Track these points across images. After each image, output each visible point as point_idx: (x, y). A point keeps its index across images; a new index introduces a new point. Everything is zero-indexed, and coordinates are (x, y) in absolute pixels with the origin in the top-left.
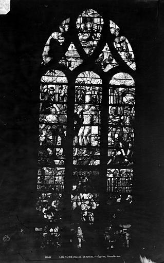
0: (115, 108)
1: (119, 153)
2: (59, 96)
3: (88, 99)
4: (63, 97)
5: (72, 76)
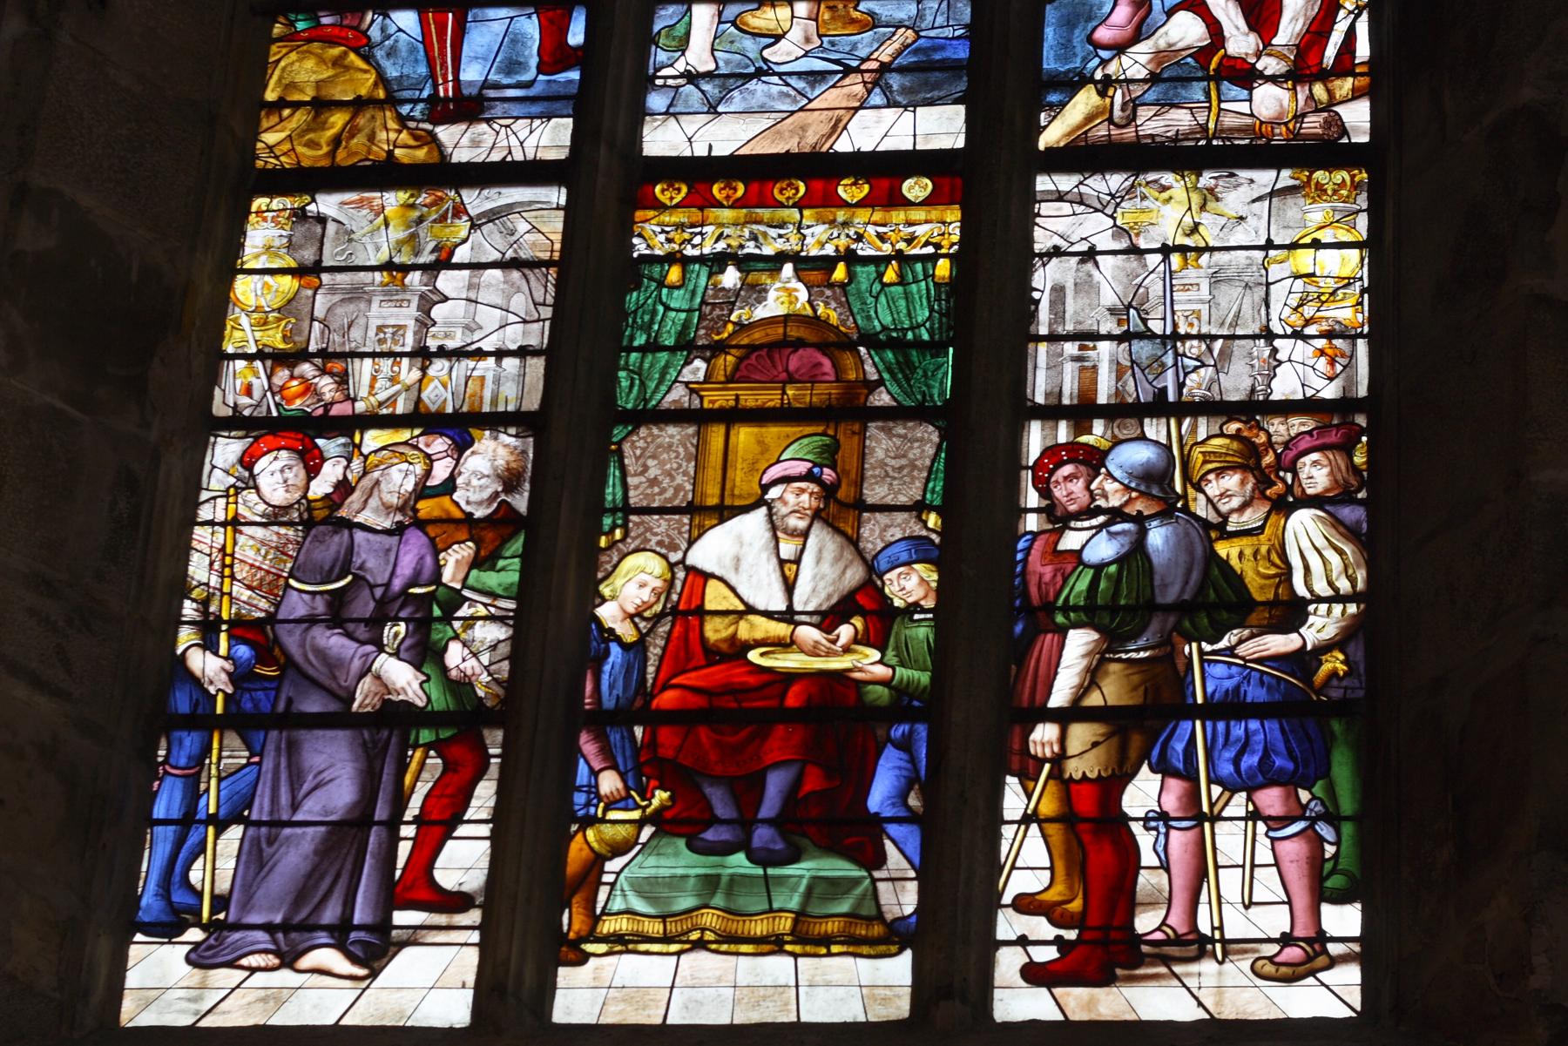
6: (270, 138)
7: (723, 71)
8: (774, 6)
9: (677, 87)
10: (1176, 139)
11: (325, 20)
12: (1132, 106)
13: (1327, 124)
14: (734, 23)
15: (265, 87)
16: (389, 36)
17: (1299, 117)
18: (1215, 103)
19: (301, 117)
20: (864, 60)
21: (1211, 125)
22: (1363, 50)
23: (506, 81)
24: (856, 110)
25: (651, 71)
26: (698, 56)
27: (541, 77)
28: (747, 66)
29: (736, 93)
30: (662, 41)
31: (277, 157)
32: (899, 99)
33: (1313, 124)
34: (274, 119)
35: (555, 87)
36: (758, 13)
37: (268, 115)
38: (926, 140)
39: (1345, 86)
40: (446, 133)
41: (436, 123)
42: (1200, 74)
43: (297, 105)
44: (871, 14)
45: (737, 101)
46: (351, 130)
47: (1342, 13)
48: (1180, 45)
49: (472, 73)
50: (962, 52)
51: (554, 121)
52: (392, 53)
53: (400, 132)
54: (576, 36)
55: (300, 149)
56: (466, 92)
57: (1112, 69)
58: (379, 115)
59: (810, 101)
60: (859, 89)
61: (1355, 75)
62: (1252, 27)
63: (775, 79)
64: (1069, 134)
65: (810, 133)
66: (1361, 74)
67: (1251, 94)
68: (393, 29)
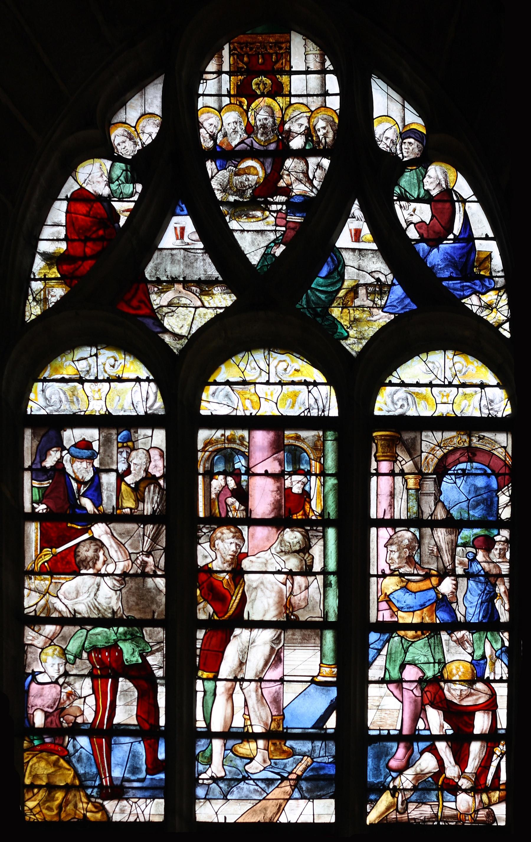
0: (406, 535)
1: (427, 763)
2: (121, 478)
3: (263, 498)
4: (138, 490)
6: (31, 804)
7: (229, 777)
8: (248, 742)
9: (209, 785)
10: (424, 821)
11: (47, 740)
12: (406, 802)
14: (231, 750)
15: (24, 776)
16: (77, 751)
17: (476, 811)
18: (441, 803)
19: (42, 794)
20: (290, 773)
21: (439, 814)
23: (133, 778)
24: (288, 800)
25: (197, 775)
26: (216, 769)
27: (148, 777)
28: (239, 775)
29: (235, 789)
31: (34, 815)
32: (306, 795)
34: (31, 794)
35: (155, 782)
36: (242, 745)
37: (27, 792)
38: (319, 818)
39: (495, 795)
40: (109, 805)
41: (104, 800)
42: (434, 787)
43: (40, 787)
44: (292, 748)
45: (235, 794)
46: (65, 802)
47: (495, 757)
48: (426, 771)
49: (117, 773)
50: (332, 771)
51: (156, 800)
52: (79, 760)
53: (88, 804)
54: (161, 755)
55: (44, 811)
56: (115, 783)
57: (397, 782)
58: (78, 794)
59: (268, 794)
60: (288, 789)
61: (500, 790)
62: (457, 762)
63: (251, 782)
64: (379, 817)
65: (268, 812)
66: (503, 790)
67: (456, 798)
68: (78, 747)
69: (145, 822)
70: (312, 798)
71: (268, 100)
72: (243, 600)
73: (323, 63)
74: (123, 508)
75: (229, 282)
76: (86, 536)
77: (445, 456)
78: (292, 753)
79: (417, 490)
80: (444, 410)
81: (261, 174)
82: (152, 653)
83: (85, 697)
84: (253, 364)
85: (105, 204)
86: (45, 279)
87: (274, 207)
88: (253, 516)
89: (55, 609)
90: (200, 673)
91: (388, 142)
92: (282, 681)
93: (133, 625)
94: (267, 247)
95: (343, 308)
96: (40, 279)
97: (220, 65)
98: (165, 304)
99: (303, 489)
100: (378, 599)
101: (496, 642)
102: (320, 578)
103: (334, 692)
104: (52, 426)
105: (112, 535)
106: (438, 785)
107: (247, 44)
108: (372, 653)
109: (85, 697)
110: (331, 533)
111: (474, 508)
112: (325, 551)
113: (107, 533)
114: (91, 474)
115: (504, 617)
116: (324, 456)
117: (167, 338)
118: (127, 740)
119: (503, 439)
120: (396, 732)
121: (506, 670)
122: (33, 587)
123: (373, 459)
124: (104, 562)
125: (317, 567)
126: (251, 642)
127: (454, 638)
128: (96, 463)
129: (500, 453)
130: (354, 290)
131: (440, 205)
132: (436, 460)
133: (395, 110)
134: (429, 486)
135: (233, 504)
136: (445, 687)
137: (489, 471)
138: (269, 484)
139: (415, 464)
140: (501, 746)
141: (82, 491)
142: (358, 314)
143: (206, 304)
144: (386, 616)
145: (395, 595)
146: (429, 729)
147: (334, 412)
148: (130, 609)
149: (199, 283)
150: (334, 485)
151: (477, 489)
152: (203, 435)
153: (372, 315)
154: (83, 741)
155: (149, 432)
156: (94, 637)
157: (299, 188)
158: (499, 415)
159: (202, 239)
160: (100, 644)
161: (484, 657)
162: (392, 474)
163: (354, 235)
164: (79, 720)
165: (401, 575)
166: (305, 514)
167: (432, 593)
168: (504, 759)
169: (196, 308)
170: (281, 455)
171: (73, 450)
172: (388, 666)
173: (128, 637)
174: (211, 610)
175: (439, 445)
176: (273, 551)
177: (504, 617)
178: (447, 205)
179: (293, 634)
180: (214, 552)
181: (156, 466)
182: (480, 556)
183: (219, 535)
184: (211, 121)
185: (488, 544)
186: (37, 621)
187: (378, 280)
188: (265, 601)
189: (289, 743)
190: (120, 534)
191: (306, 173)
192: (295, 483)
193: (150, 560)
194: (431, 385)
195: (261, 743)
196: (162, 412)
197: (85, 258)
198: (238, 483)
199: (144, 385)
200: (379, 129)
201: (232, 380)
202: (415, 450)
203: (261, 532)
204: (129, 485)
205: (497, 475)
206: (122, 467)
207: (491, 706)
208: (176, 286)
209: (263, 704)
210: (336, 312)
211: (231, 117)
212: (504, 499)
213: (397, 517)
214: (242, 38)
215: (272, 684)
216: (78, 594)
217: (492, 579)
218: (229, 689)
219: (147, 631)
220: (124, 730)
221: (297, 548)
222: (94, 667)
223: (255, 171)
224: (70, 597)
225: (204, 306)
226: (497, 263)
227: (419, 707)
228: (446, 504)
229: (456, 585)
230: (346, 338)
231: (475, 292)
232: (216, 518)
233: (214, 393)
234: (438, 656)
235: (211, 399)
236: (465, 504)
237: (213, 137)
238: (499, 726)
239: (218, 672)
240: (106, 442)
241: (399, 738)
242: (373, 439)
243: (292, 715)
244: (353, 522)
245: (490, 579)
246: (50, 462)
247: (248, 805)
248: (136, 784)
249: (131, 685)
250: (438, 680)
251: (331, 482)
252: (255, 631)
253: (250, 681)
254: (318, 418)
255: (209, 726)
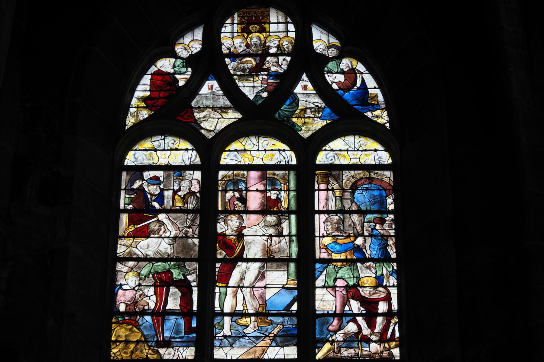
0: (335, 218)
1: (352, 327)
2: (175, 193)
3: (254, 201)
4: (184, 199)
5: (210, 150)
11: (126, 318)
12: (339, 348)
13: (389, 354)
14: (235, 322)
17: (382, 352)
19: (122, 345)
22: (397, 334)
23: (176, 336)
24: (269, 347)
26: (227, 331)
29: (237, 342)
30: (217, 327)
33: (385, 354)
34: (115, 346)
37: (113, 344)
39: (393, 344)
40: (162, 351)
43: (120, 342)
44: (271, 320)
46: (135, 349)
47: (391, 324)
48: (351, 332)
49: (167, 334)
50: (295, 332)
54: (194, 324)
57: (334, 337)
60: (269, 341)
61: (395, 341)
63: (247, 338)
69: (183, 359)
70: (283, 346)
71: (258, 34)
72: (243, 249)
73: (286, 19)
74: (175, 206)
75: (236, 107)
76: (155, 219)
77: (356, 181)
78: (272, 323)
79: (341, 197)
80: (353, 161)
81: (254, 63)
82: (190, 274)
83: (150, 296)
84: (250, 142)
85: (171, 76)
86: (138, 107)
87: (261, 76)
88: (249, 210)
89: (135, 254)
90: (218, 284)
91: (321, 50)
92: (265, 287)
93: (179, 261)
94: (257, 93)
95: (298, 118)
96: (135, 107)
97: (233, 20)
98: (202, 117)
99: (277, 197)
100: (320, 247)
101: (389, 267)
102: (287, 238)
103: (296, 293)
104: (138, 170)
105: (169, 219)
106: (359, 338)
107: (247, 12)
108: (317, 274)
109: (150, 296)
110: (293, 217)
111: (373, 205)
112: (290, 225)
113: (166, 218)
114: (158, 191)
115: (394, 256)
116: (288, 182)
117: (203, 132)
118: (174, 317)
119: (387, 173)
120: (332, 312)
121: (396, 281)
122: (123, 243)
123: (316, 183)
124: (164, 232)
125: (286, 232)
126: (247, 269)
127: (365, 266)
128: (162, 186)
129: (387, 180)
130: (304, 110)
131: (349, 75)
132: (351, 184)
133: (324, 37)
134: (348, 195)
135: (237, 204)
136: (361, 290)
137: (381, 188)
138: (259, 195)
139: (340, 185)
140: (395, 319)
141: (153, 199)
142: (306, 120)
143: (224, 117)
144: (325, 255)
145: (330, 245)
146: (352, 310)
147: (294, 162)
148: (178, 253)
149: (220, 108)
150: (294, 195)
151: (374, 196)
152: (221, 173)
153: (314, 120)
154: (148, 318)
155: (192, 172)
156: (157, 267)
157: (273, 69)
158: (386, 163)
159: (222, 90)
160: (159, 271)
161: (382, 275)
162: (327, 190)
163: (304, 88)
164: (146, 308)
165: (333, 236)
166: (278, 208)
167: (351, 245)
168: (397, 325)
169: (219, 118)
170: (265, 182)
171: (149, 181)
172: (327, 280)
173: (176, 267)
174: (225, 253)
175: (352, 177)
176: (260, 225)
177: (394, 256)
178: (353, 75)
179: (272, 265)
180: (227, 227)
181: (195, 187)
182: (378, 227)
183: (229, 218)
184: (228, 42)
185: (382, 221)
186: (124, 260)
187: (317, 106)
188: (256, 249)
189: (269, 318)
190: (174, 219)
191: (278, 63)
192: (273, 195)
193: (191, 230)
194: (347, 150)
195: (253, 318)
196: (199, 163)
197: (159, 98)
198: (241, 195)
199: (190, 152)
200: (315, 45)
201: (238, 149)
202: (339, 179)
203: (253, 217)
204: (180, 196)
205: (385, 190)
206: (176, 188)
207: (388, 299)
208: (208, 109)
209: (254, 299)
210: (294, 120)
211: (238, 41)
212: (390, 200)
213: (330, 209)
214: (244, 10)
215: (260, 289)
216: (148, 246)
217: (385, 238)
218: (234, 292)
219: (187, 264)
220: (173, 313)
221: (274, 224)
222: (156, 281)
223: (251, 62)
224: (144, 248)
225: (223, 118)
226: (381, 98)
227: (346, 299)
228: (357, 203)
229: (365, 241)
230: (301, 130)
231: (370, 111)
232: (228, 210)
233: (228, 155)
234: (356, 275)
235: (227, 158)
236: (369, 203)
237: (229, 49)
238: (393, 309)
239: (228, 283)
240: (167, 177)
241: (334, 315)
242: (316, 174)
243: (271, 304)
244: (305, 212)
245: (384, 238)
246: (136, 185)
247: (245, 350)
248: (178, 340)
249: (177, 290)
250: (356, 286)
251: (292, 194)
252: (250, 264)
253: (247, 287)
254: (285, 165)
255: (222, 310)
